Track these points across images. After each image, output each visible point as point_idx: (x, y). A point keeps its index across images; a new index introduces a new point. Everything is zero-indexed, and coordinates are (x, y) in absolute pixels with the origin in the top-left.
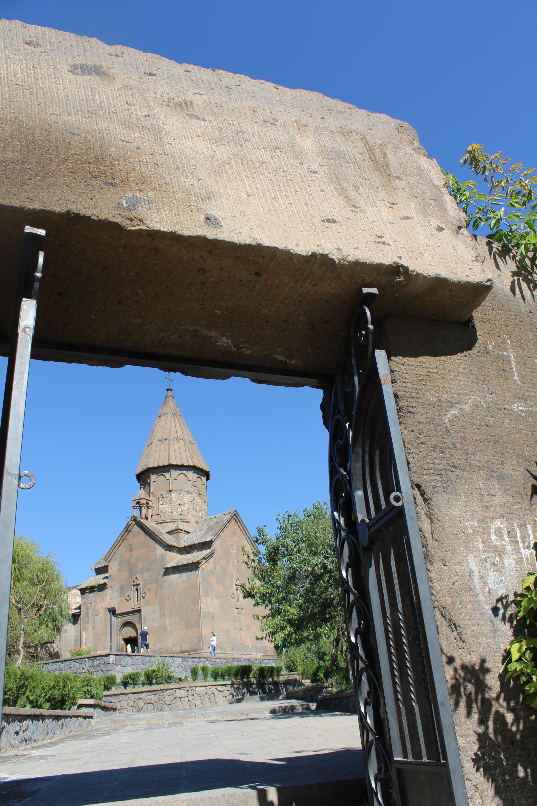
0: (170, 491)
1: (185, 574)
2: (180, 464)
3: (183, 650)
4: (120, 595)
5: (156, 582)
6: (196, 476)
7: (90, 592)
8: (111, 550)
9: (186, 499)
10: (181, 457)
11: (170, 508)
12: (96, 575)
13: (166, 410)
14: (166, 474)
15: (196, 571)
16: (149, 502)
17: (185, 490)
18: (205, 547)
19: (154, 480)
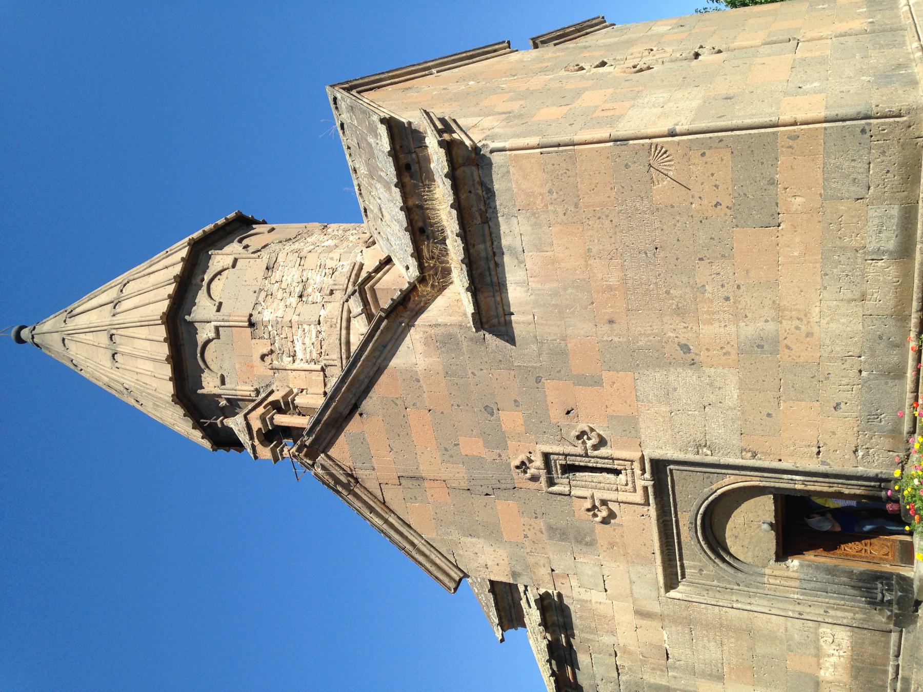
0: (252, 325)
1: (503, 229)
2: (171, 289)
3: (890, 242)
4: (587, 544)
5: (538, 380)
6: (234, 248)
7: (574, 665)
8: (421, 559)
9: (289, 274)
10: (157, 287)
11: (305, 326)
12: (524, 626)
13: (54, 342)
14: (202, 337)
15: (490, 164)
16: (271, 399)
17: (260, 277)
18: (419, 162)
19: (218, 382)
